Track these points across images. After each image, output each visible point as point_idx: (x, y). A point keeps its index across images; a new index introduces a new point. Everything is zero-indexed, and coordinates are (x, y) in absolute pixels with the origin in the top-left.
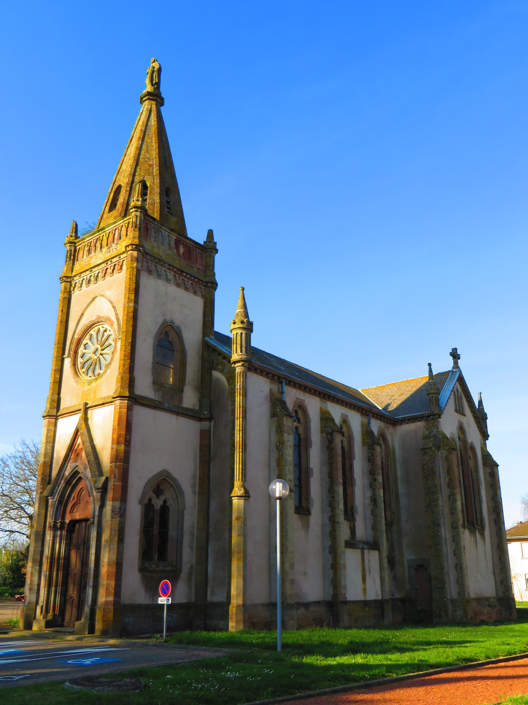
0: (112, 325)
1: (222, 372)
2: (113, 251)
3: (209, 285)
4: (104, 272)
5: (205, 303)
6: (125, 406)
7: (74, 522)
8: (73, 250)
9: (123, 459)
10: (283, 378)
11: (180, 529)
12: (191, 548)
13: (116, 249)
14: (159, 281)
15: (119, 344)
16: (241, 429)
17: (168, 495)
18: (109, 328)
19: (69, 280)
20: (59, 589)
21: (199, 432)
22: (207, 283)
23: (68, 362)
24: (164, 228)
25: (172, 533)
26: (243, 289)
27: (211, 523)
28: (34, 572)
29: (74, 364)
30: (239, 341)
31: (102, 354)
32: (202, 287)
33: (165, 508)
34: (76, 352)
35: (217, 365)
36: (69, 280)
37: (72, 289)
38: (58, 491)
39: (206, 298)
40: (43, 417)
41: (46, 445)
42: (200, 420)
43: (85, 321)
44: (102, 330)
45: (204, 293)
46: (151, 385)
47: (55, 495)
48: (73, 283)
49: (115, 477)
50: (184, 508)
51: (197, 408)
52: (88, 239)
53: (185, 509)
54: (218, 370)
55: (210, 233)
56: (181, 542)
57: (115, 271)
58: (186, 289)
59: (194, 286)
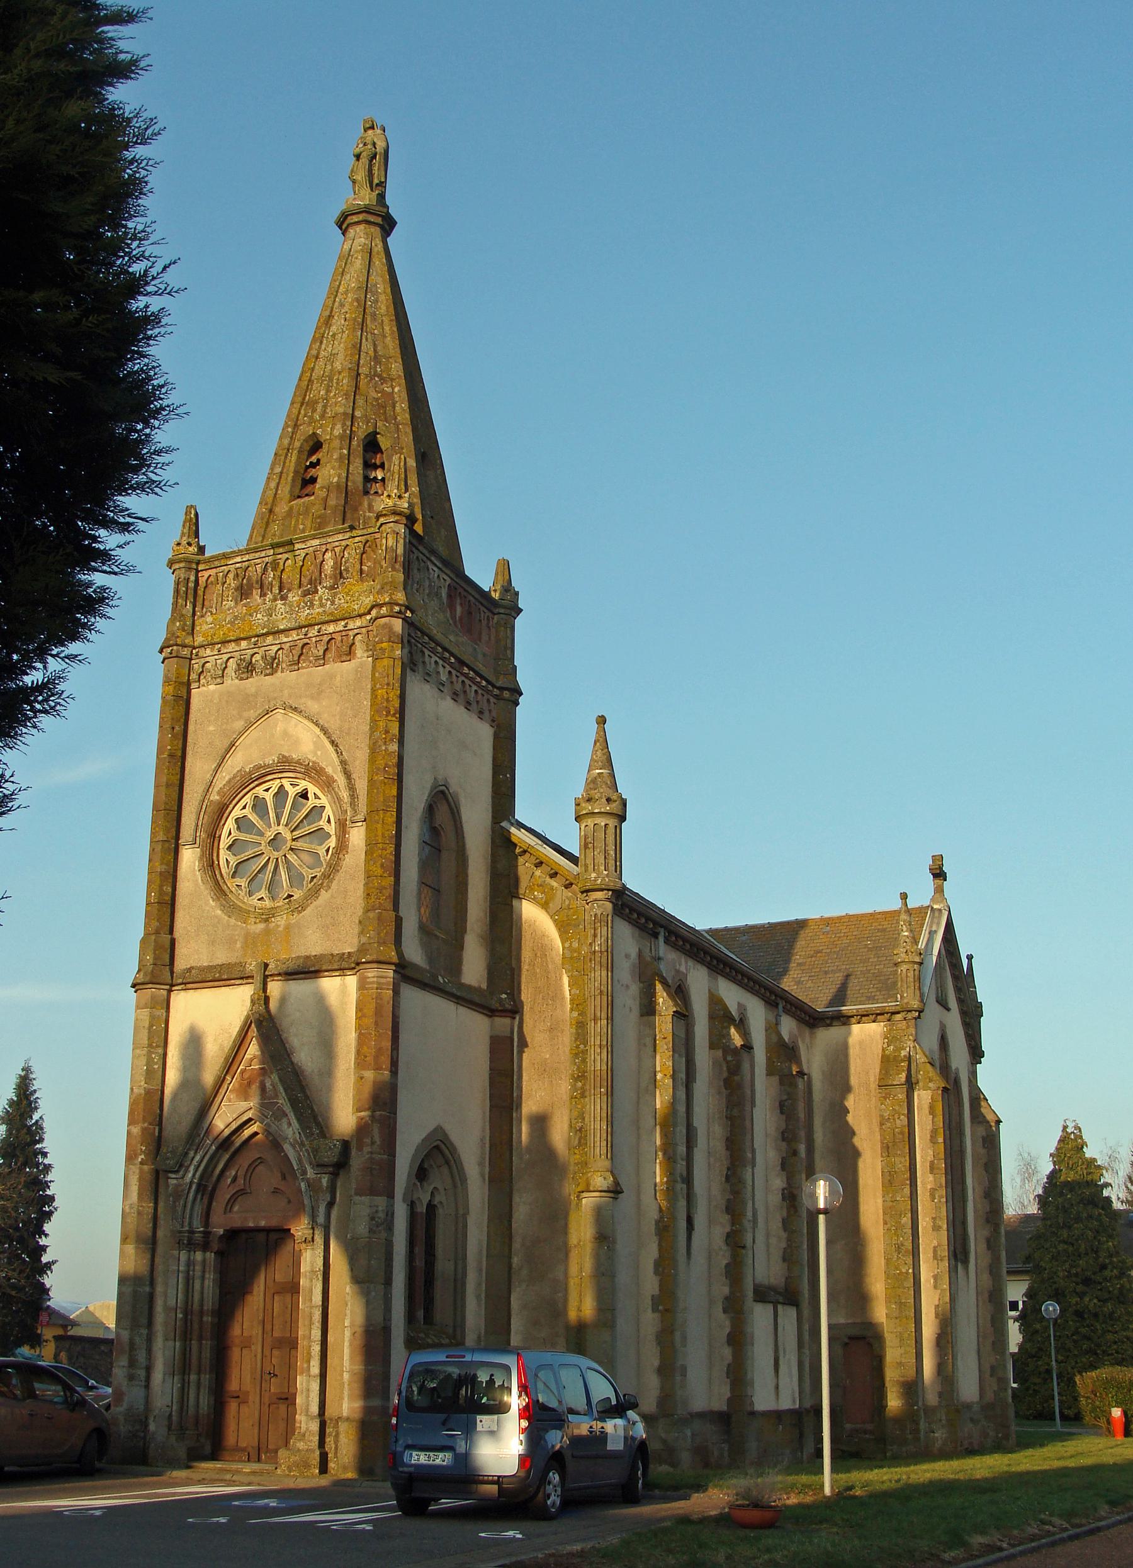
0: (327, 784)
1: (545, 906)
2: (322, 605)
3: (506, 694)
4: (297, 652)
5: (496, 736)
6: (387, 983)
7: (232, 1234)
8: (192, 578)
9: (383, 1103)
10: (662, 926)
11: (460, 1258)
12: (478, 1297)
13: (333, 603)
14: (427, 687)
15: (357, 836)
16: (604, 1043)
17: (439, 1179)
18: (312, 789)
19: (186, 652)
20: (206, 1378)
21: (487, 1041)
22: (501, 689)
23: (189, 857)
24: (421, 548)
25: (444, 1265)
26: (602, 720)
27: (517, 1245)
28: (137, 1340)
29: (210, 864)
30: (600, 844)
31: (291, 849)
32: (492, 700)
33: (431, 1207)
34: (213, 836)
35: (532, 890)
36: (186, 652)
37: (193, 676)
38: (195, 1162)
39: (498, 726)
40: (133, 986)
41: (149, 1053)
42: (491, 1012)
43: (238, 762)
44: (292, 792)
45: (494, 714)
46: (416, 933)
47: (187, 1171)
48: (196, 665)
49: (373, 1143)
50: (466, 1213)
51: (484, 986)
52: (239, 559)
53: (468, 1213)
54: (535, 900)
55: (504, 567)
56: (464, 1284)
57: (329, 655)
58: (468, 705)
59: (480, 697)
